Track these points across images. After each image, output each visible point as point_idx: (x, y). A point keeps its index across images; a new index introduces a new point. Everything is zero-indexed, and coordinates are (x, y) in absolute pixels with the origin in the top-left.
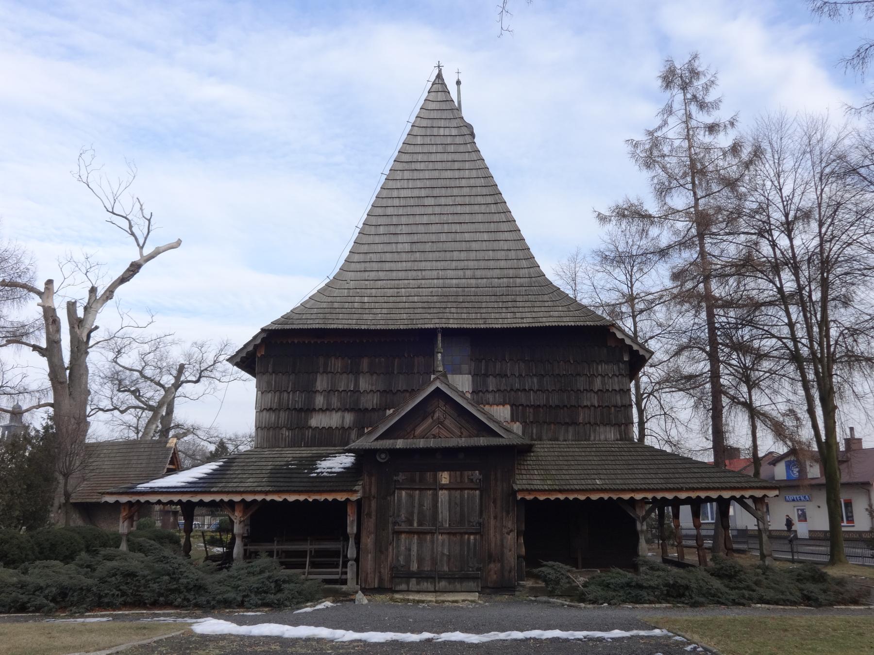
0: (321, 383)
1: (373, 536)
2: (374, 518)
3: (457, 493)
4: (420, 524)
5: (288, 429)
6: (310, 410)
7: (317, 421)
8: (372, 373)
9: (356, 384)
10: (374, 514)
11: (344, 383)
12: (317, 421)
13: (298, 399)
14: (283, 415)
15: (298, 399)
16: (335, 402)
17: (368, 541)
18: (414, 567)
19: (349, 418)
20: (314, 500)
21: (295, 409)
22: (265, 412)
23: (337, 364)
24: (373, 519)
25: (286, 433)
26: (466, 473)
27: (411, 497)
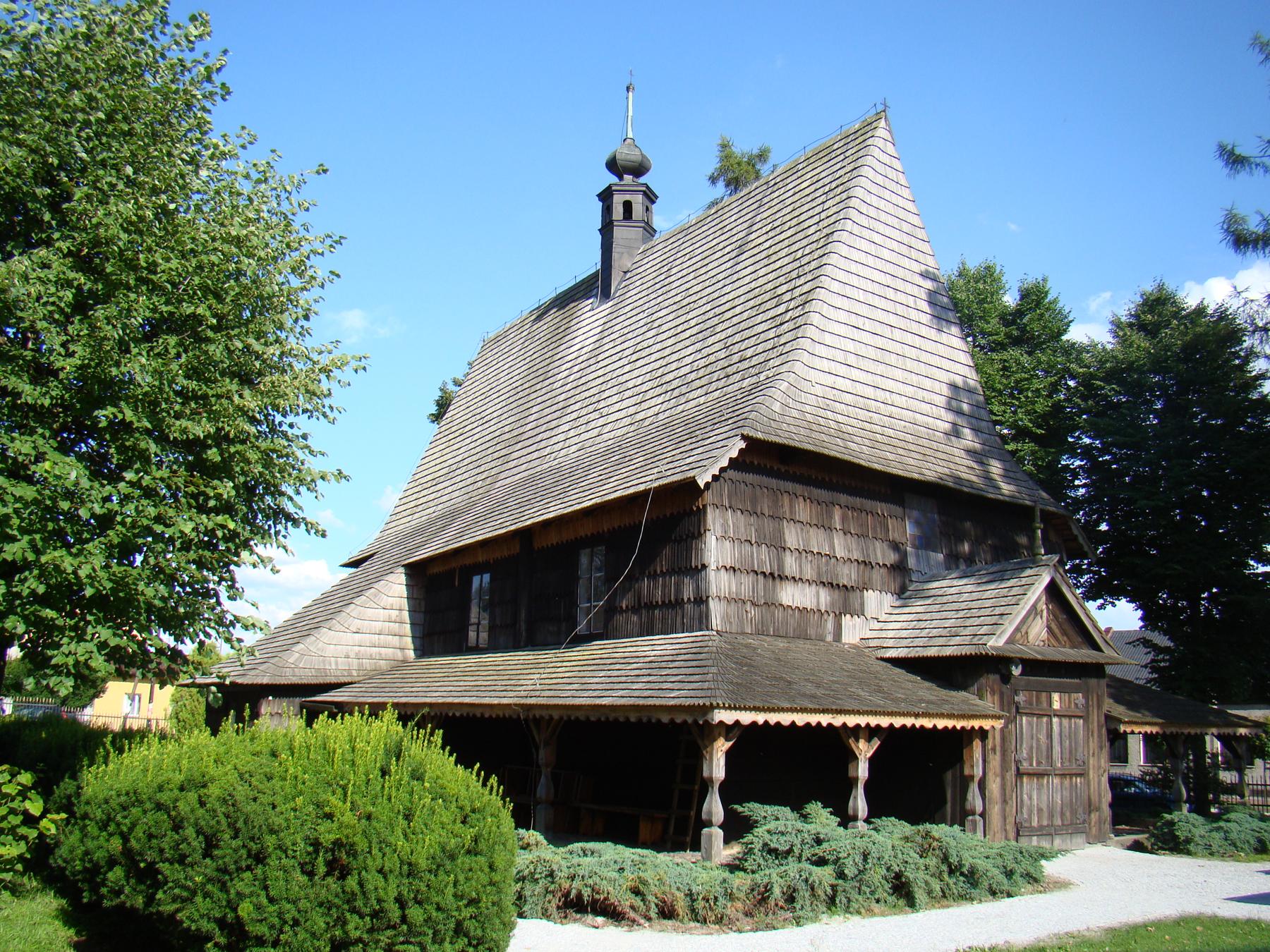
0: (792, 537)
1: (998, 780)
2: (998, 753)
3: (1065, 721)
4: (1039, 763)
5: (753, 604)
6: (777, 576)
7: (791, 595)
8: (846, 532)
9: (832, 547)
10: (998, 748)
11: (817, 541)
12: (791, 595)
13: (763, 558)
14: (747, 580)
15: (763, 558)
16: (809, 573)
17: (994, 786)
18: (1035, 824)
19: (824, 598)
20: (963, 728)
21: (764, 573)
22: (723, 570)
23: (803, 510)
24: (998, 757)
25: (753, 612)
26: (1074, 695)
27: (1030, 724)
